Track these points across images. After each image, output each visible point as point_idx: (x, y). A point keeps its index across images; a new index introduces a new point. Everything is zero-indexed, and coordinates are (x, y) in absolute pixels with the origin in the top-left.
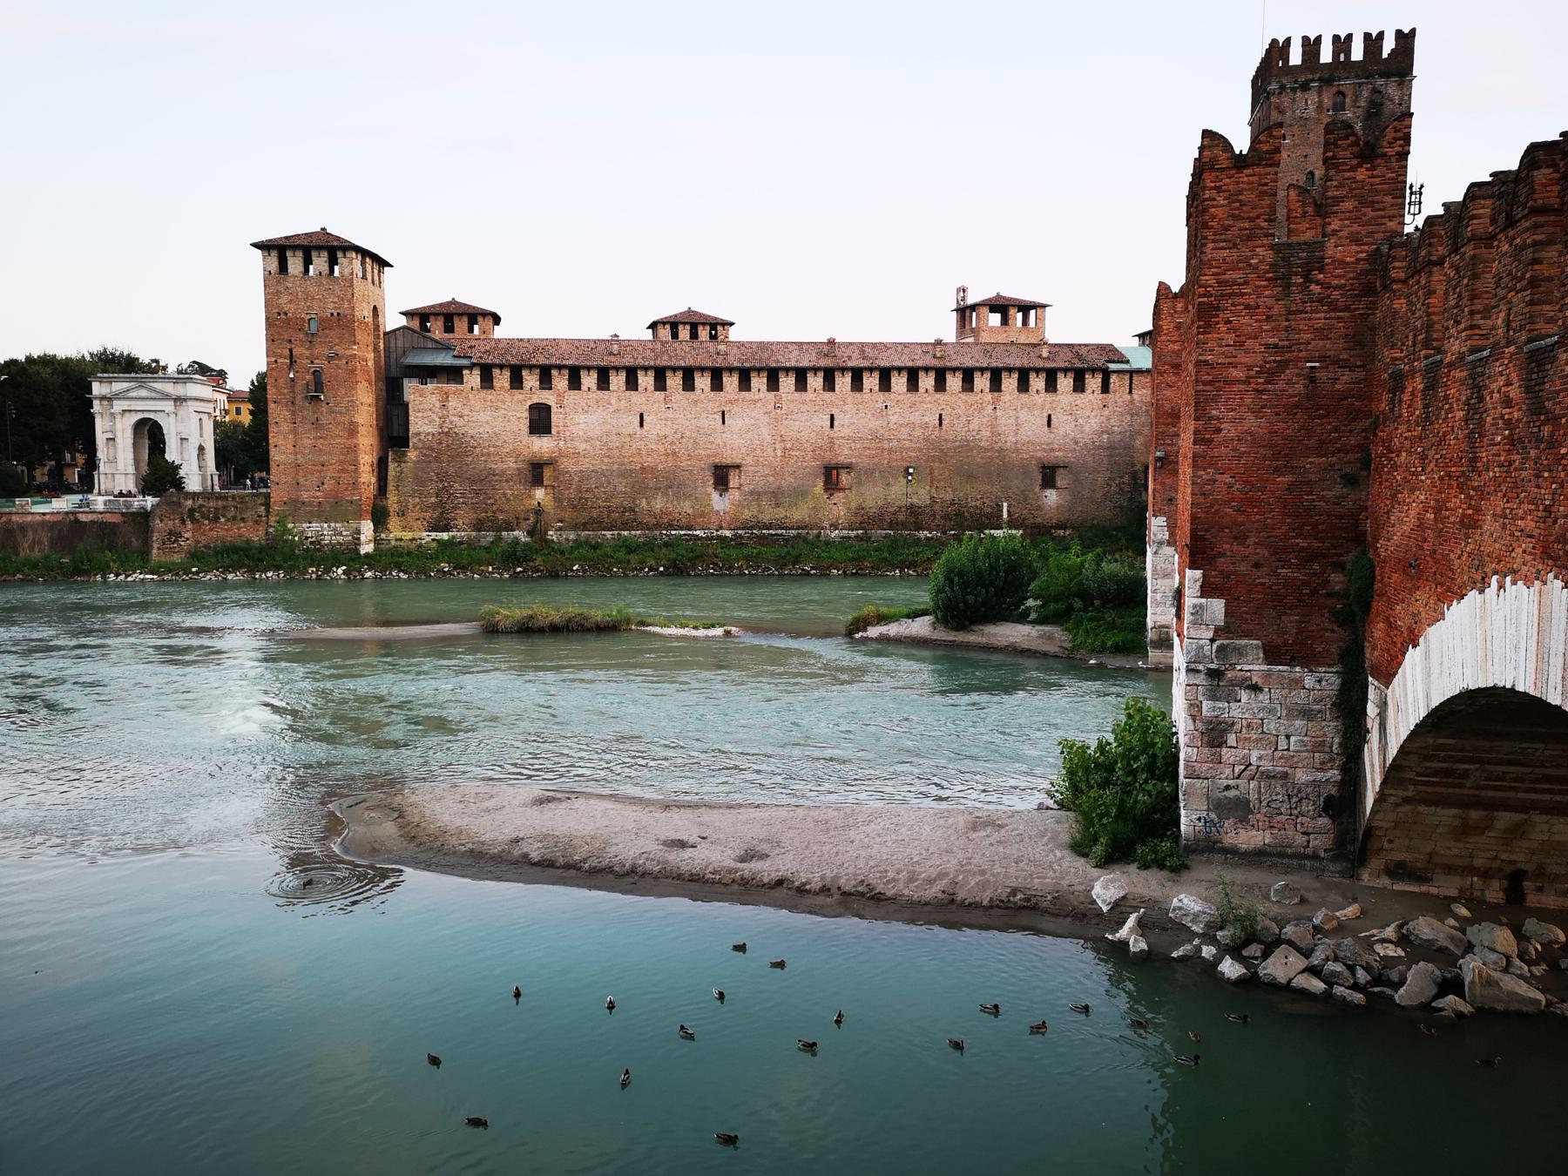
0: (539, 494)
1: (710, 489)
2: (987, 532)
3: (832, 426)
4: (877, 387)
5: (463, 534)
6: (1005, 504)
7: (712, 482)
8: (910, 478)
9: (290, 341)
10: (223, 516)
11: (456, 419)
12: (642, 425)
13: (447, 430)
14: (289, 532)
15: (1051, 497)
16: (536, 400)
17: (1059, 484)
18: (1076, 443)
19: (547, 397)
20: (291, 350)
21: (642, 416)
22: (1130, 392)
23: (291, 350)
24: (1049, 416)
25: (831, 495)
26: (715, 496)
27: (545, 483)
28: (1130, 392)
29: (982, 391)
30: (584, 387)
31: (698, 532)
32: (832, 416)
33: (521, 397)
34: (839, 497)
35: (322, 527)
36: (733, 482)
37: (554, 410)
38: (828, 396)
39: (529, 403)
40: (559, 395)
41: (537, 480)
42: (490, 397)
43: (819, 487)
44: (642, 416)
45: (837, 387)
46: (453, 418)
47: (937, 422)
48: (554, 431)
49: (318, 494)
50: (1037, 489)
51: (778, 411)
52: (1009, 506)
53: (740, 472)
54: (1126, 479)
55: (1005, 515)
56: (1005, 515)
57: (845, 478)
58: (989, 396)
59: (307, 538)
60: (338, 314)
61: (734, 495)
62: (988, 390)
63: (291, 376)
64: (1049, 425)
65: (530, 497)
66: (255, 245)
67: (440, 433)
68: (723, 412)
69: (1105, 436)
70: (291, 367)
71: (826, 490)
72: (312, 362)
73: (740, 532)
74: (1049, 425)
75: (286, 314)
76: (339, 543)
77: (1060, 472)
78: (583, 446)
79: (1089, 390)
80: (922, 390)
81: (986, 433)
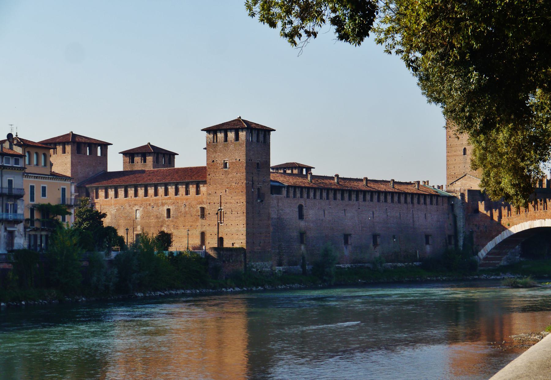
0: (303, 247)
1: (343, 245)
2: (414, 263)
3: (373, 218)
4: (384, 201)
5: (286, 267)
6: (418, 251)
7: (343, 242)
8: (395, 240)
9: (252, 173)
10: (232, 260)
11: (281, 211)
12: (324, 216)
13: (279, 217)
14: (252, 267)
15: (428, 248)
16: (300, 203)
17: (430, 242)
18: (432, 225)
19: (302, 202)
20: (253, 177)
21: (324, 211)
22: (443, 205)
23: (253, 177)
24: (425, 214)
25: (375, 247)
26: (345, 248)
27: (305, 242)
28: (443, 205)
29: (409, 203)
30: (311, 198)
31: (341, 265)
32: (373, 212)
33: (296, 201)
34: (378, 248)
35: (261, 264)
36: (349, 242)
37: (304, 208)
38: (371, 203)
39: (298, 205)
40: (305, 201)
41: (302, 242)
42: (289, 201)
43: (371, 245)
44: (324, 211)
45: (374, 201)
46: (281, 211)
47: (399, 216)
48: (305, 217)
49: (259, 248)
50: (425, 245)
51: (359, 210)
52: (419, 252)
53: (351, 237)
54: (444, 241)
55: (418, 257)
56: (418, 257)
57: (379, 240)
58: (411, 205)
59: (258, 269)
60: (266, 161)
61: (350, 247)
62: (410, 203)
63: (253, 190)
64: (426, 218)
65: (300, 249)
67: (278, 218)
68: (345, 210)
69: (439, 223)
70: (253, 187)
71: (374, 245)
72: (258, 184)
73: (352, 265)
74: (426, 218)
75: (251, 160)
76: (267, 272)
77: (430, 238)
78: (312, 225)
79: (434, 204)
80: (395, 202)
81: (411, 221)
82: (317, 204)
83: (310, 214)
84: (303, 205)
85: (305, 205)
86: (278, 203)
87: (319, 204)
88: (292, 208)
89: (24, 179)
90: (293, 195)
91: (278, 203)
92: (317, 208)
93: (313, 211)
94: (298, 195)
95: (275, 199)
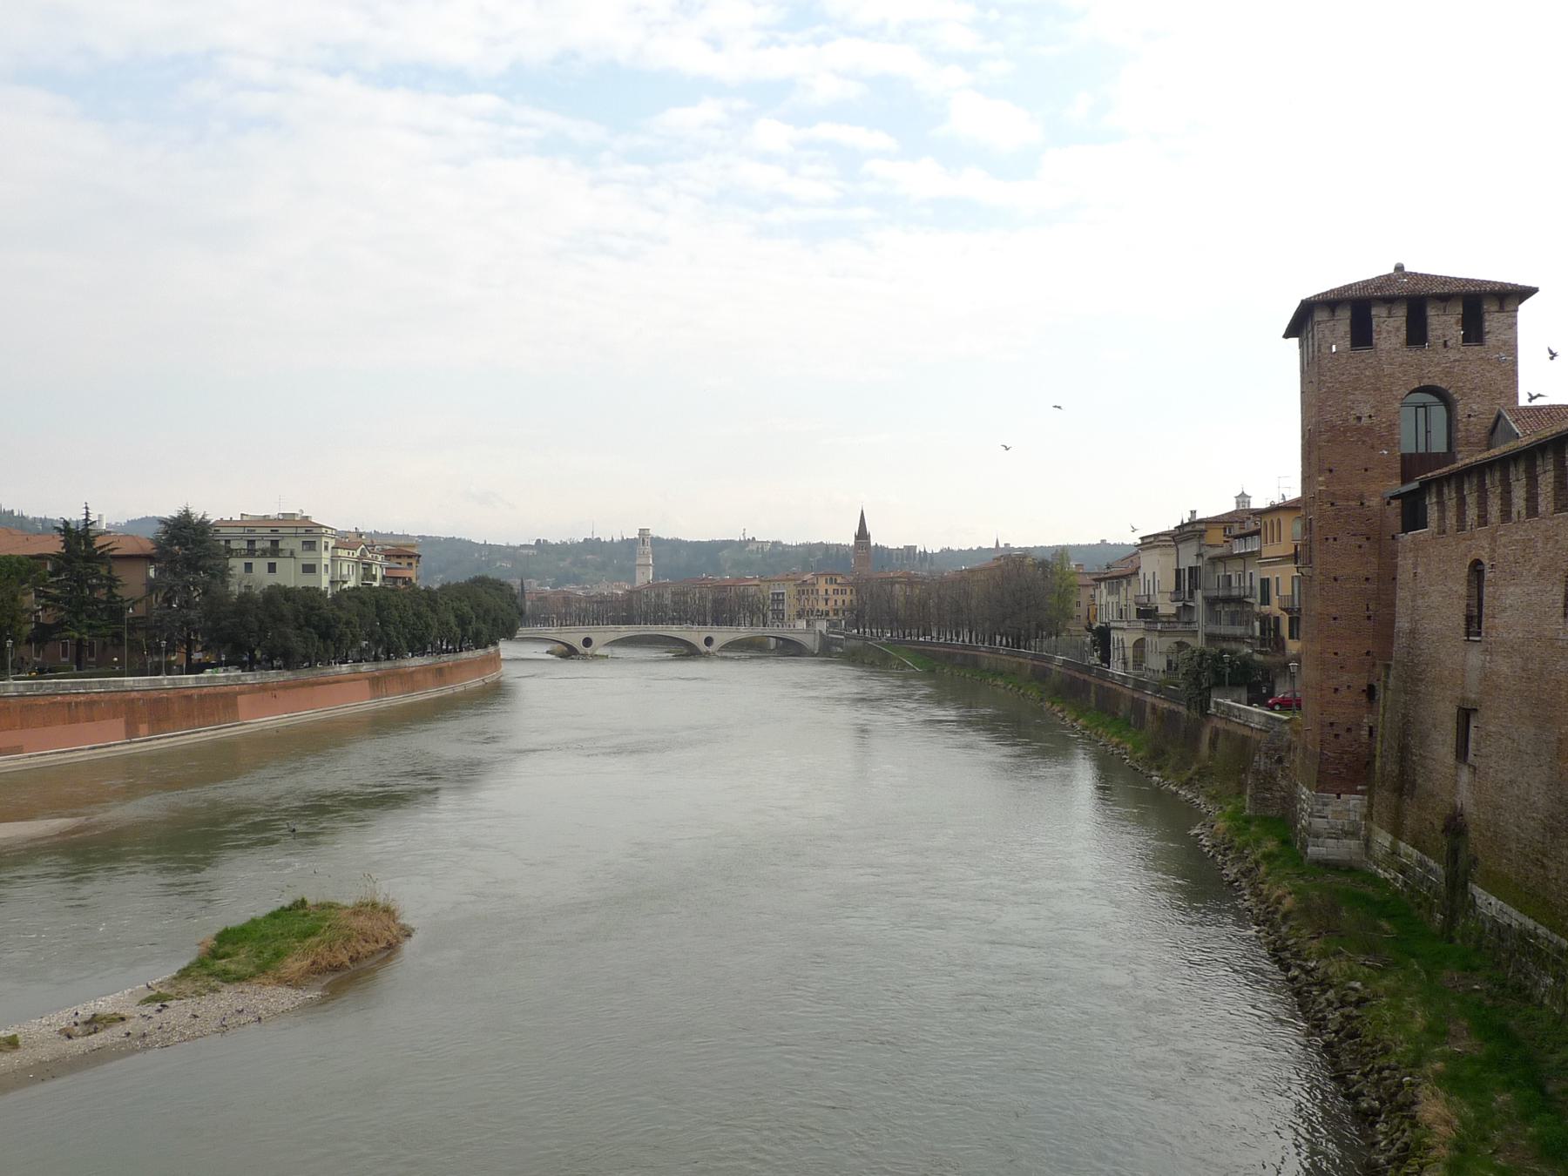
16: (1474, 555)
39: (1468, 564)
40: (1494, 539)
66: (1287, 336)
82: (1539, 545)
83: (1504, 610)
84: (1485, 561)
85: (1491, 559)
86: (1415, 565)
87: (1548, 539)
88: (1450, 584)
89: (1262, 568)
90: (1454, 522)
91: (1415, 565)
92: (1536, 571)
93: (1518, 590)
94: (1472, 513)
95: (1410, 551)
